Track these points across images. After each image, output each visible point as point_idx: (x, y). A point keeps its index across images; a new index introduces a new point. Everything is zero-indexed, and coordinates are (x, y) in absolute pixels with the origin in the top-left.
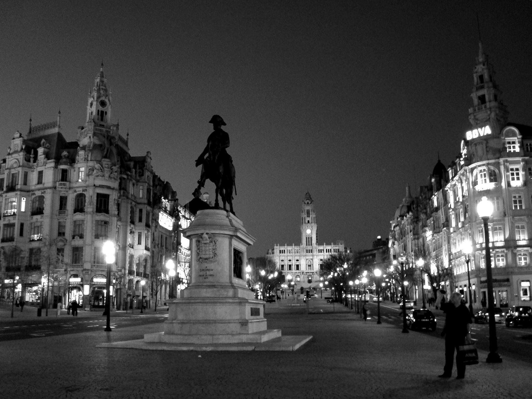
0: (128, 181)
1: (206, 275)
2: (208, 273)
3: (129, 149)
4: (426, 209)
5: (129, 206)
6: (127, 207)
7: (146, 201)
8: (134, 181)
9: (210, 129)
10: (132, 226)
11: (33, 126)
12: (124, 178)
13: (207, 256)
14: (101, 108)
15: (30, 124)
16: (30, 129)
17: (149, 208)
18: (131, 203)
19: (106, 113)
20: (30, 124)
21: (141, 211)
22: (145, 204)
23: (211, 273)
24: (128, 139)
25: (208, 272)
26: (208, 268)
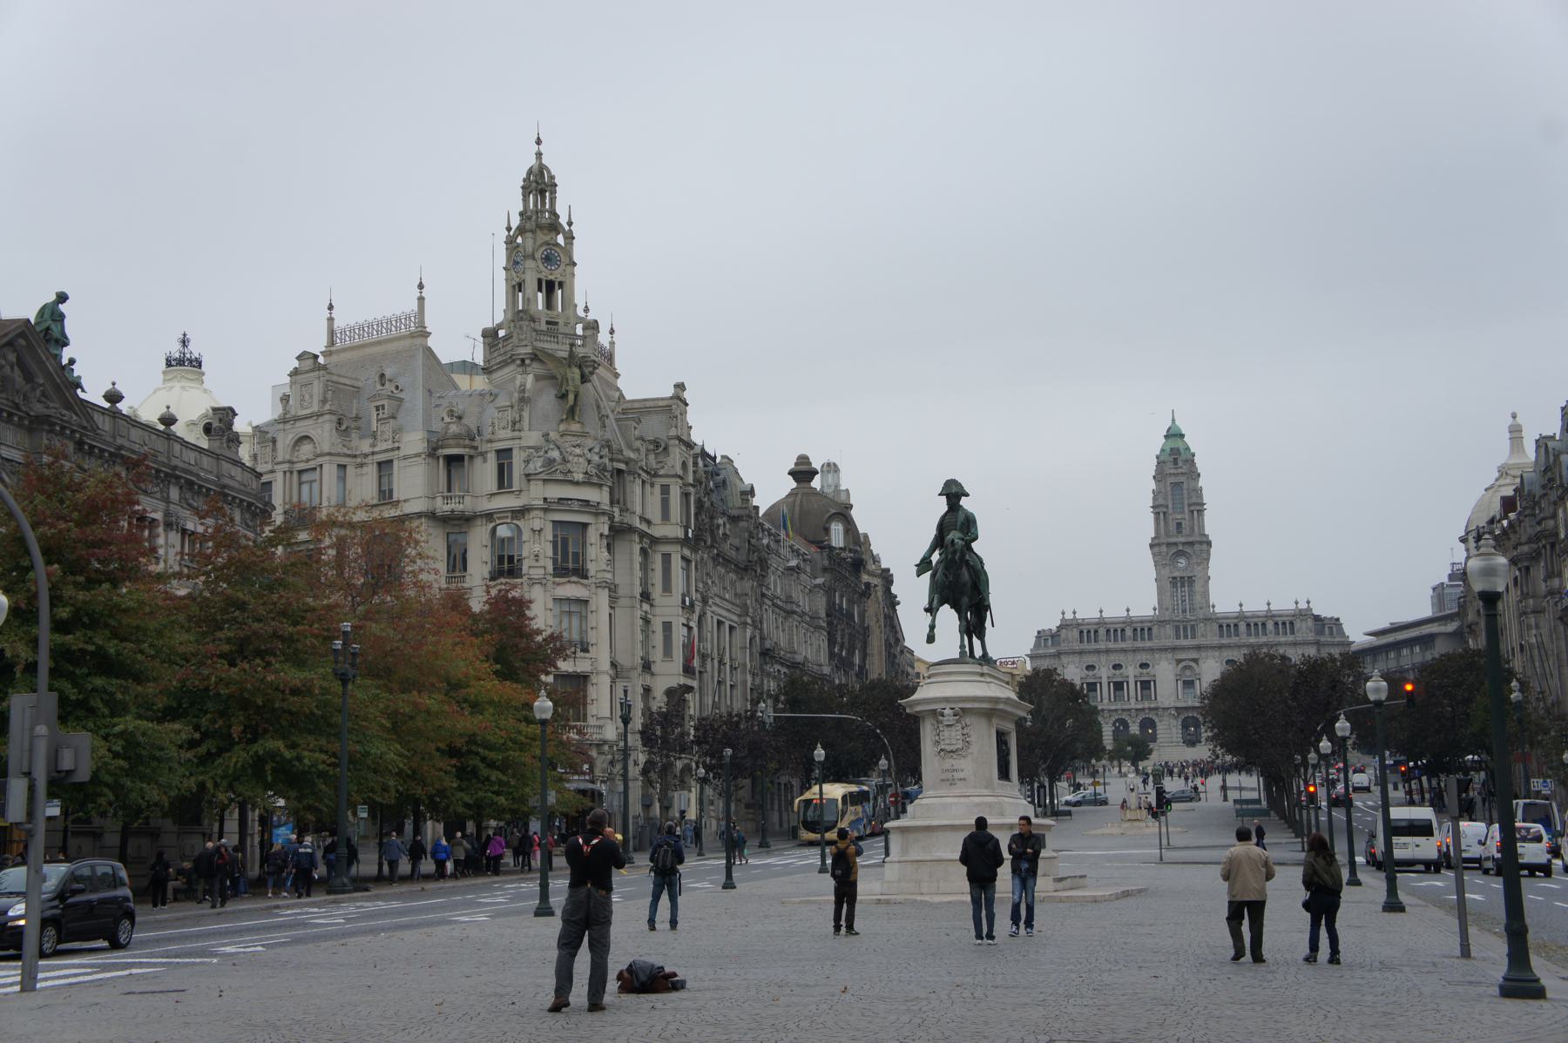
0: (629, 478)
3: (617, 376)
4: (1554, 516)
5: (637, 548)
6: (631, 554)
7: (681, 534)
8: (644, 475)
9: (942, 506)
10: (646, 607)
11: (339, 324)
12: (620, 472)
13: (954, 748)
14: (546, 275)
15: (331, 320)
16: (332, 333)
17: (687, 552)
19: (561, 285)
20: (331, 320)
21: (667, 558)
22: (675, 541)
23: (961, 775)
24: (612, 343)
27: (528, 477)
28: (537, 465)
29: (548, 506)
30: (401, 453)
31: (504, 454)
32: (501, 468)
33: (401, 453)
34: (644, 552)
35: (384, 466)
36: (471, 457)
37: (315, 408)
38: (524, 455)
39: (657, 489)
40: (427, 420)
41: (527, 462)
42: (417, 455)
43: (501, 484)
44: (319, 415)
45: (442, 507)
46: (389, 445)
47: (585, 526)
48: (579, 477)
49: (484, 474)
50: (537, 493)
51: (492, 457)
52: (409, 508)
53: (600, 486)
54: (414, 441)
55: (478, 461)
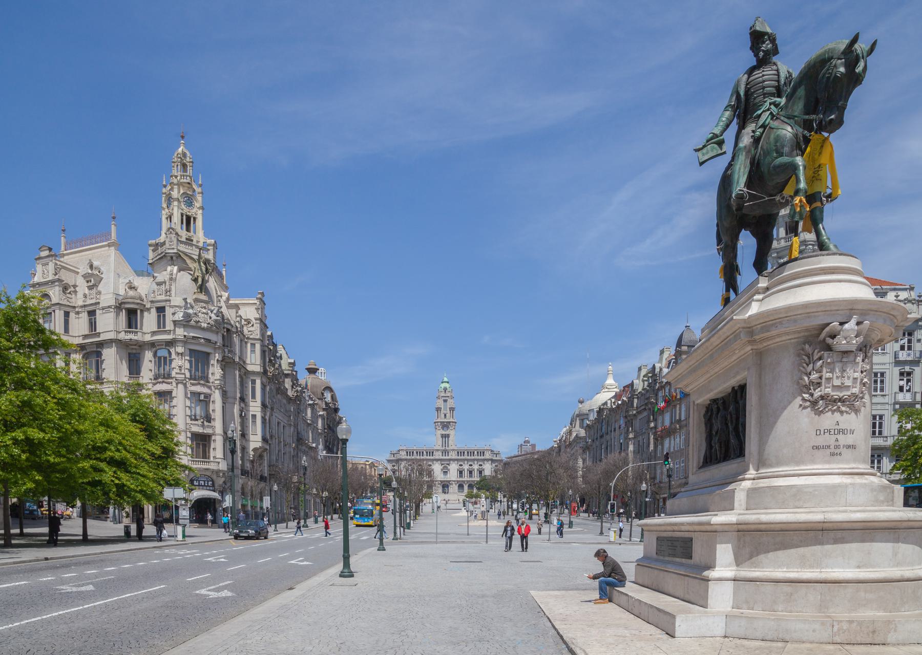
1: (837, 447)
2: (843, 440)
18: (240, 371)
25: (841, 437)
26: (841, 426)
27: (175, 323)
28: (179, 316)
29: (186, 341)
30: (101, 305)
31: (161, 310)
32: (159, 317)
33: (101, 305)
34: (240, 376)
35: (92, 313)
36: (142, 311)
37: (51, 277)
38: (172, 310)
39: (249, 345)
40: (116, 287)
41: (174, 314)
42: (109, 307)
43: (159, 327)
44: (53, 282)
45: (122, 336)
46: (93, 301)
47: (208, 354)
48: (204, 325)
49: (149, 321)
50: (180, 332)
51: (154, 311)
52: (103, 337)
53: (217, 333)
54: (107, 299)
55: (146, 314)
